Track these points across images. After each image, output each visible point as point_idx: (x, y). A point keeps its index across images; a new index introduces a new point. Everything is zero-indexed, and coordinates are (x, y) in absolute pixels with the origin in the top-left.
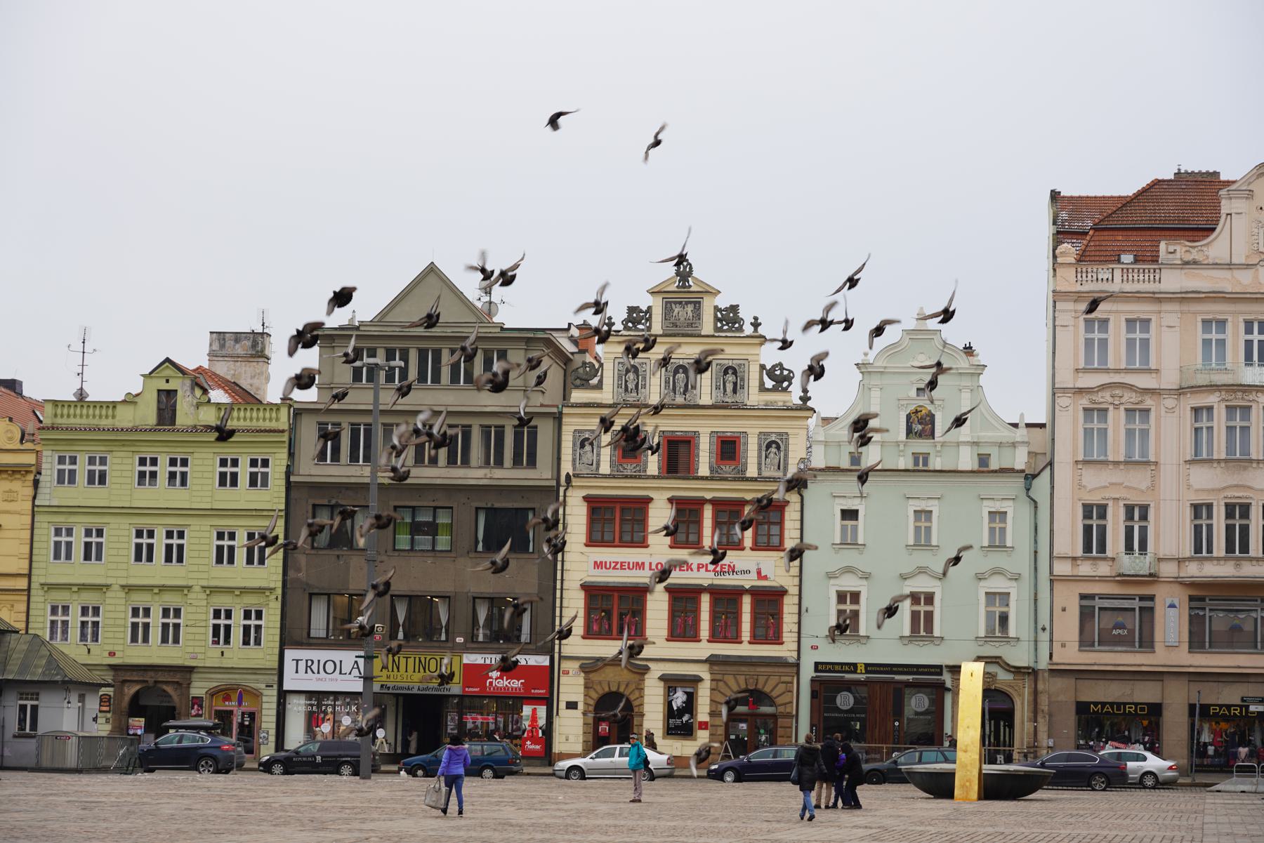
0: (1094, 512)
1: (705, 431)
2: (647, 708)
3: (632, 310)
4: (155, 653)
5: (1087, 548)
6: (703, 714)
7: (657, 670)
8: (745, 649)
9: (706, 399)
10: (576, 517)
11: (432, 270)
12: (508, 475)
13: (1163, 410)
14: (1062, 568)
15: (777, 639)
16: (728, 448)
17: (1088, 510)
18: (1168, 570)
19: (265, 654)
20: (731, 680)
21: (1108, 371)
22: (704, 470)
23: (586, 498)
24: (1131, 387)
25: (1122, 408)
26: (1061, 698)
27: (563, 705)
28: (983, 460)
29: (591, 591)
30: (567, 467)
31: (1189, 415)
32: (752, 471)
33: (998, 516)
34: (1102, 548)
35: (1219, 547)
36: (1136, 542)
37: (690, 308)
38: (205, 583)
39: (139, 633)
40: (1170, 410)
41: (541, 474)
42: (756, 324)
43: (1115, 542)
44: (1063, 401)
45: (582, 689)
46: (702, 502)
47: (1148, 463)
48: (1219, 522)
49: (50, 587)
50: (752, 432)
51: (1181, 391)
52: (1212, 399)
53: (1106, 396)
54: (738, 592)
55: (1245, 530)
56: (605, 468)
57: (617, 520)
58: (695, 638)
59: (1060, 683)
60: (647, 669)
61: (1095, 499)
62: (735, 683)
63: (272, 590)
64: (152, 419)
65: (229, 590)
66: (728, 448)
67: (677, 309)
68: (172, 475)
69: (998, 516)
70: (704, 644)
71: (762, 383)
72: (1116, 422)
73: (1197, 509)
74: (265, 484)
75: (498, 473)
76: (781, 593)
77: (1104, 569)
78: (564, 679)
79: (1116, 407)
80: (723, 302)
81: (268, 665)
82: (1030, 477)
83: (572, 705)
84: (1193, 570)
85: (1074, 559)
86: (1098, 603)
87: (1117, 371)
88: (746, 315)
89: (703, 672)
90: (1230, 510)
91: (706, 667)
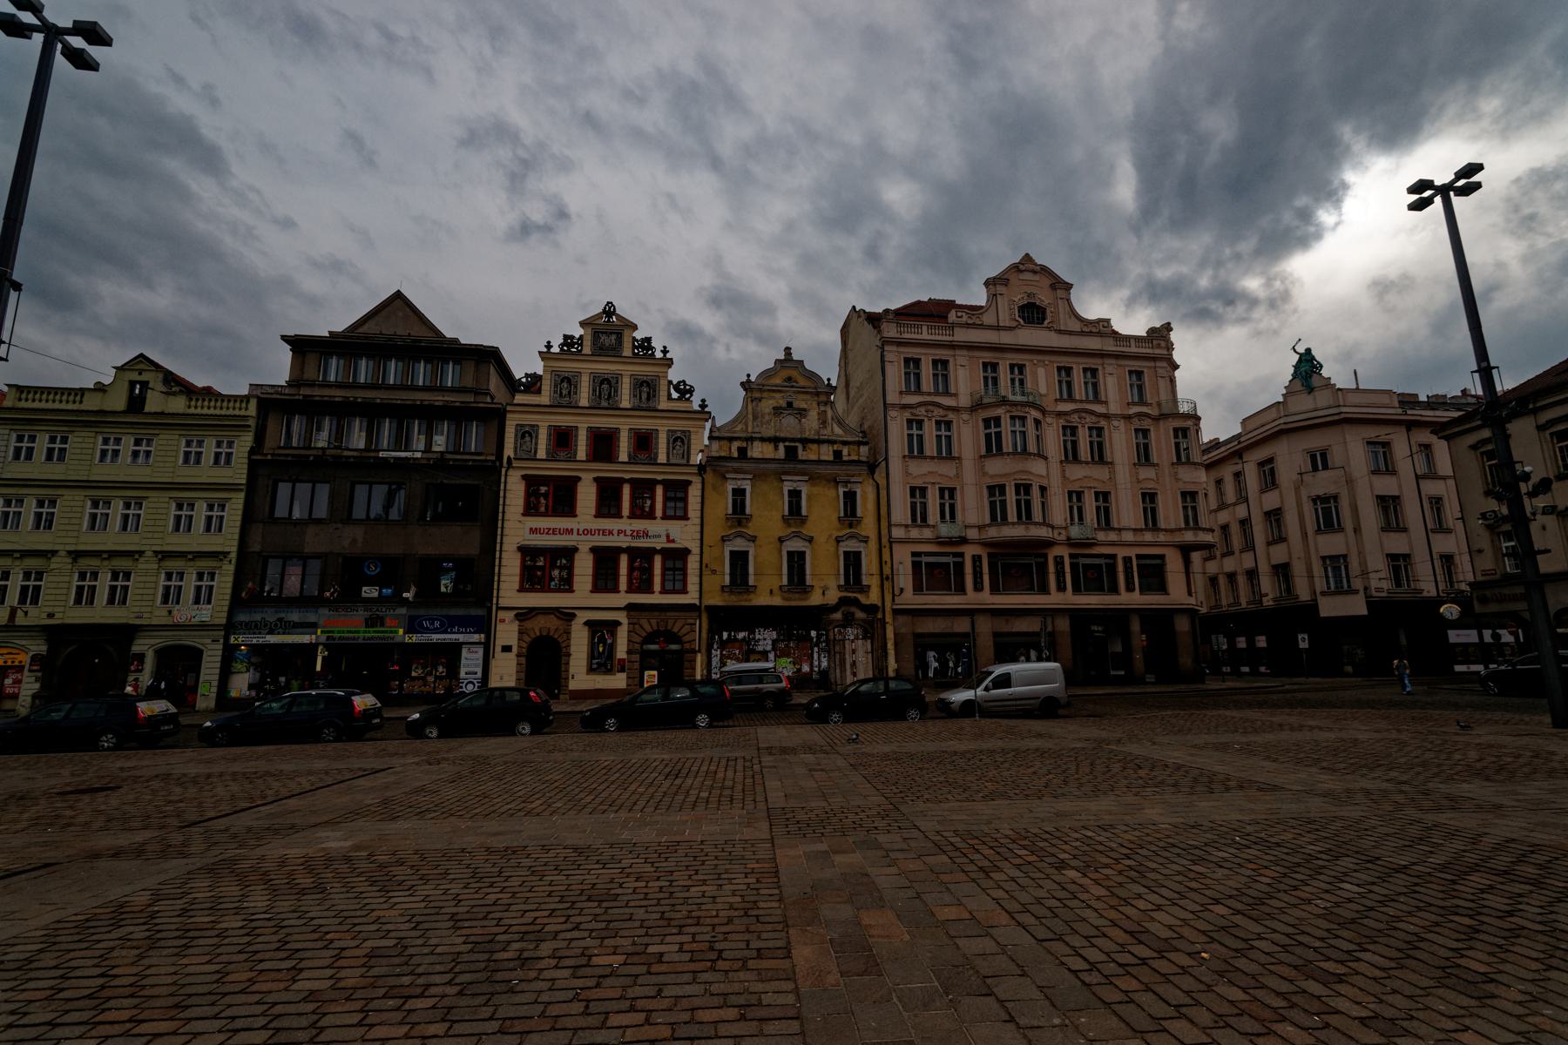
0: (918, 492)
1: (625, 427)
2: (573, 649)
3: (566, 337)
4: (100, 613)
5: (914, 519)
6: (621, 652)
7: (583, 617)
8: (656, 598)
9: (625, 404)
10: (514, 491)
11: (398, 295)
14: (898, 533)
15: (684, 591)
16: (644, 442)
17: (913, 490)
18: (972, 534)
20: (644, 623)
21: (923, 394)
22: (623, 457)
23: (524, 477)
24: (939, 405)
26: (903, 630)
27: (498, 649)
28: (838, 454)
29: (525, 551)
30: (509, 451)
31: (981, 424)
32: (662, 458)
34: (924, 519)
35: (1012, 515)
36: (949, 512)
37: (613, 337)
38: (158, 548)
39: (84, 596)
42: (665, 351)
43: (933, 516)
45: (515, 635)
46: (622, 481)
47: (954, 458)
48: (1011, 497)
50: (663, 429)
52: (1000, 411)
53: (922, 410)
54: (649, 553)
56: (542, 454)
57: (554, 496)
58: (616, 590)
59: (901, 619)
60: (574, 615)
61: (918, 483)
62: (648, 624)
63: (226, 554)
65: (181, 555)
66: (644, 442)
67: (603, 337)
68: (135, 454)
70: (623, 594)
71: (669, 395)
73: (991, 489)
74: (228, 462)
76: (686, 552)
77: (927, 533)
78: (500, 627)
80: (639, 335)
81: (217, 621)
82: (872, 467)
83: (507, 649)
84: (993, 533)
85: (907, 526)
86: (925, 559)
87: (929, 394)
88: (657, 345)
89: (622, 617)
90: (1017, 487)
91: (624, 614)
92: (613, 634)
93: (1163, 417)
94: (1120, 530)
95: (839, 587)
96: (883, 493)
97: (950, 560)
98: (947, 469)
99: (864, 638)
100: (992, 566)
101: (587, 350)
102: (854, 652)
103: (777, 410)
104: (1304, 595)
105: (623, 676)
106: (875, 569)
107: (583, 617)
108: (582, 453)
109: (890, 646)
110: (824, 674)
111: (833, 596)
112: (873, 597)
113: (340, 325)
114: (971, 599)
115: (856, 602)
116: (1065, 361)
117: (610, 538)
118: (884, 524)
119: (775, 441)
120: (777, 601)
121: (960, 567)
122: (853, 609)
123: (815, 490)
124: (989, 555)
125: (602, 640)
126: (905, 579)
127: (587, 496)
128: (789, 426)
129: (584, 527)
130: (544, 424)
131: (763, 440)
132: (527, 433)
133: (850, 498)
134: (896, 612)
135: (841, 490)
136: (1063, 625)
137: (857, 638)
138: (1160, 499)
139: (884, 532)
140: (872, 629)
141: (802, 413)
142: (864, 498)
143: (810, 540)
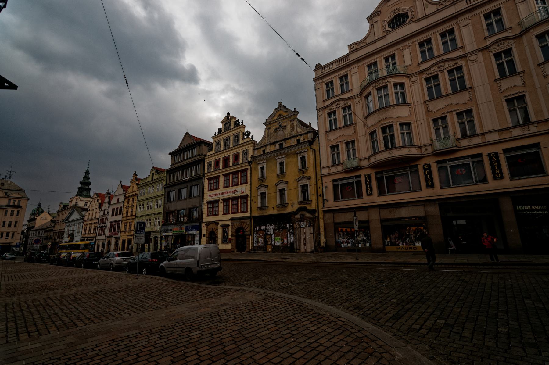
0: (334, 148)
11: (187, 134)
13: (355, 103)
14: (325, 171)
18: (365, 163)
19: (158, 228)
25: (340, 108)
26: (329, 221)
28: (299, 141)
30: (206, 172)
35: (382, 146)
40: (358, 102)
43: (343, 157)
44: (320, 113)
49: (138, 217)
51: (361, 94)
59: (327, 215)
61: (334, 143)
62: (237, 226)
72: (340, 114)
76: (246, 196)
77: (340, 168)
79: (338, 109)
82: (311, 143)
83: (204, 235)
85: (328, 167)
86: (340, 182)
88: (240, 121)
89: (229, 223)
90: (384, 129)
92: (228, 229)
93: (525, 31)
94: (483, 134)
95: (298, 202)
96: (317, 153)
97: (354, 180)
99: (310, 226)
100: (380, 181)
101: (223, 131)
102: (305, 233)
103: (276, 130)
105: (230, 244)
106: (314, 192)
107: (221, 223)
108: (221, 167)
109: (322, 230)
110: (292, 244)
111: (296, 207)
112: (313, 206)
113: (177, 147)
114: (366, 200)
115: (305, 209)
117: (227, 195)
118: (318, 168)
119: (275, 143)
120: (275, 212)
121: (359, 183)
122: (305, 213)
123: (289, 160)
124: (376, 173)
125: (226, 232)
126: (329, 195)
128: (281, 135)
130: (213, 160)
131: (270, 144)
132: (210, 164)
133: (303, 159)
134: (324, 212)
135: (299, 157)
136: (434, 210)
137: (306, 226)
138: (528, 99)
139: (318, 172)
140: (313, 223)
141: (285, 127)
142: (309, 158)
143: (287, 183)
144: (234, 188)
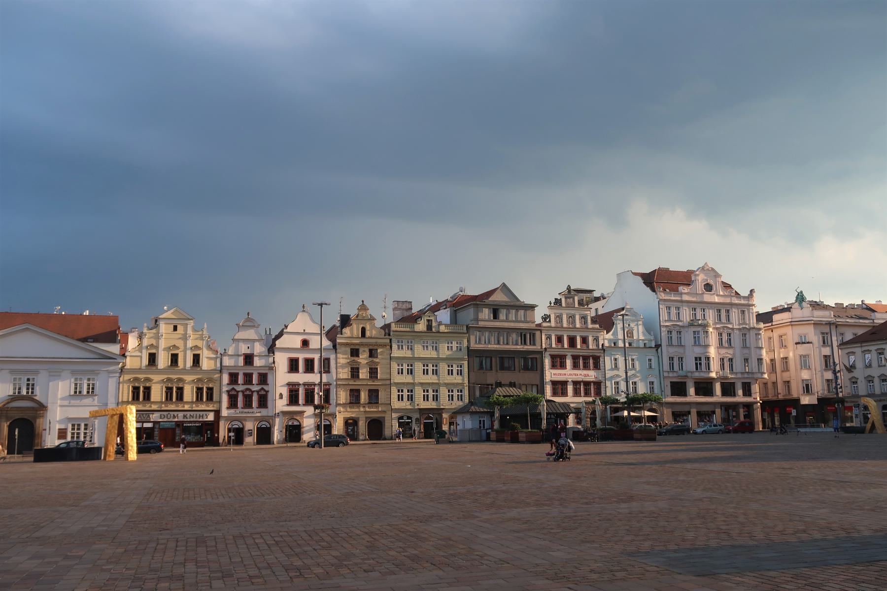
0: (671, 359)
4: (431, 404)
10: (547, 362)
12: (528, 347)
14: (666, 374)
18: (689, 375)
30: (544, 346)
33: (650, 360)
41: (537, 347)
43: (676, 367)
55: (700, 364)
57: (558, 362)
64: (425, 329)
65: (453, 384)
66: (585, 340)
69: (650, 360)
75: (526, 347)
77: (675, 375)
84: (697, 374)
98: (681, 350)
101: (564, 305)
104: (795, 395)
116: (719, 307)
127: (569, 362)
129: (568, 374)
132: (549, 337)
144: (585, 372)
